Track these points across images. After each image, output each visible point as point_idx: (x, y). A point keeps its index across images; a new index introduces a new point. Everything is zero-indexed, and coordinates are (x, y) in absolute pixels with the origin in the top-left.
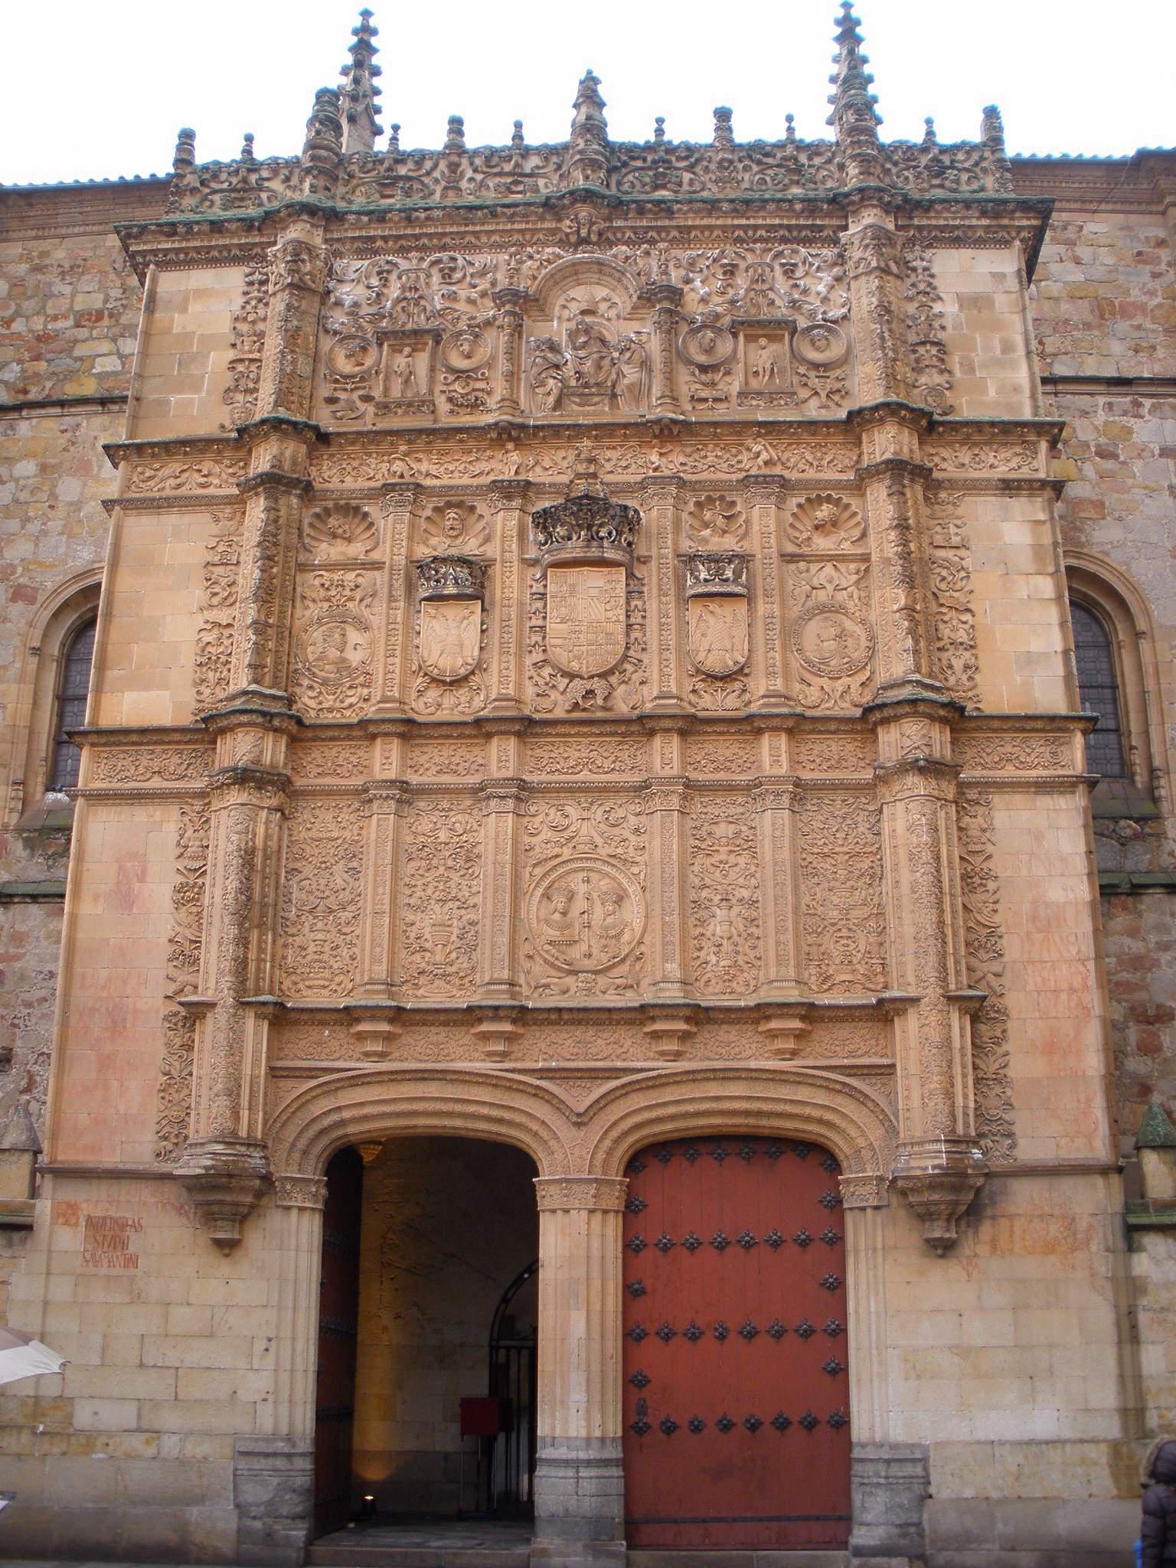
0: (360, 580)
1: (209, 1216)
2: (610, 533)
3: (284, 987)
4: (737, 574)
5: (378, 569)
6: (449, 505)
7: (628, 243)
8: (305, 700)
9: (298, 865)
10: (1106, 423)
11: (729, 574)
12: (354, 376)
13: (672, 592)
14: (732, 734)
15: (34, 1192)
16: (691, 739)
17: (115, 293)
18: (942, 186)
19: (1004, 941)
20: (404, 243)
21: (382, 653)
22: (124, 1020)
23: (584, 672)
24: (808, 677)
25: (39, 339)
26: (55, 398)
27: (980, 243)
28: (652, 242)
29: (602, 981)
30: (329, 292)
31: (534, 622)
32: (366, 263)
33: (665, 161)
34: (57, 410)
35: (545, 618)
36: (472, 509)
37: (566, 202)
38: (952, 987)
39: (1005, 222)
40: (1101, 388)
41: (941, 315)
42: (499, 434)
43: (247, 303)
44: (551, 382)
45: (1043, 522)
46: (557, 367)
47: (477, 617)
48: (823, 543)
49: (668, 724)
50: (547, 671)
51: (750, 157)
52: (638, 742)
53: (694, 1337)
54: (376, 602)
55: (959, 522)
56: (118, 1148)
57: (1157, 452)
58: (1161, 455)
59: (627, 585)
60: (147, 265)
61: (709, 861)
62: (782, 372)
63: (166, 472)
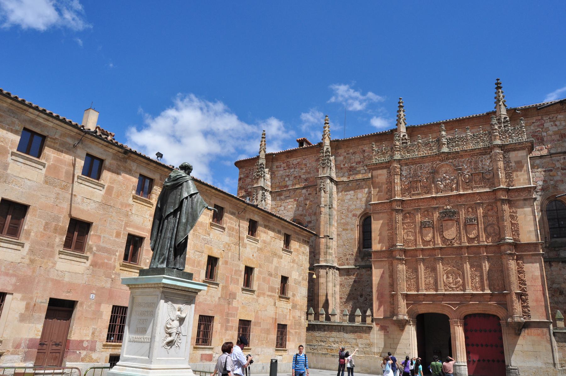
1: (399, 326)
4: (475, 221)
6: (425, 211)
7: (451, 159)
10: (563, 162)
15: (372, 321)
16: (469, 249)
17: (362, 157)
18: (511, 138)
25: (350, 167)
27: (518, 150)
28: (456, 158)
32: (407, 167)
33: (457, 141)
34: (355, 181)
39: (524, 145)
40: (562, 154)
41: (511, 166)
45: (532, 205)
47: (432, 231)
48: (490, 213)
50: (444, 239)
51: (474, 138)
53: (477, 345)
63: (379, 207)
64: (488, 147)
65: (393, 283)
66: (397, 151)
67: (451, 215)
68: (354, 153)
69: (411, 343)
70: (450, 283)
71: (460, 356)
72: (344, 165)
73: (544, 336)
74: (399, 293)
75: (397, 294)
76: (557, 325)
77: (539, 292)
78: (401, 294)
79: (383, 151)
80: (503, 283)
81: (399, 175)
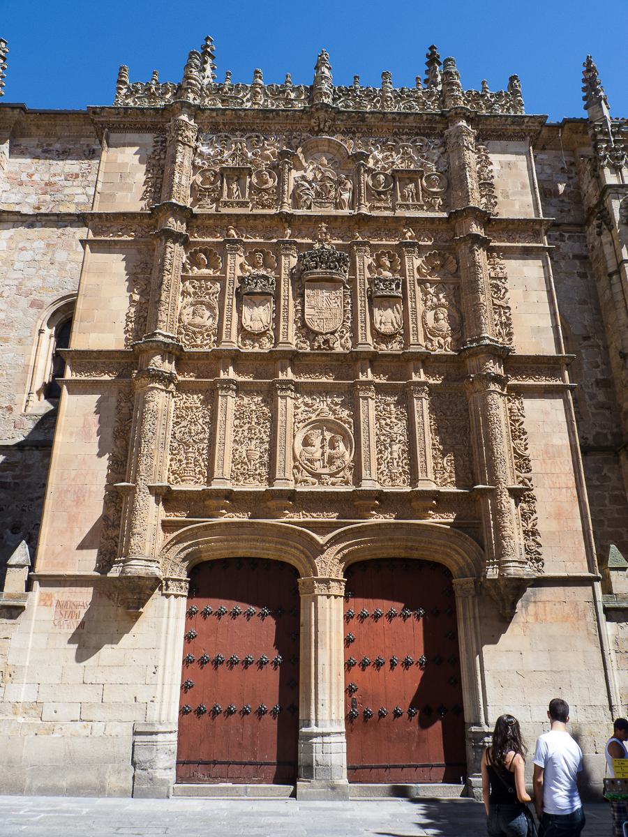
2: (336, 266)
3: (171, 480)
4: (397, 286)
6: (256, 251)
7: (343, 133)
8: (184, 340)
9: (179, 420)
11: (394, 286)
12: (210, 188)
15: (29, 587)
19: (531, 463)
22: (84, 496)
24: (431, 337)
26: (54, 212)
28: (354, 133)
29: (332, 479)
30: (196, 149)
37: (313, 109)
38: (510, 483)
39: (524, 127)
43: (155, 151)
46: (308, 189)
50: (304, 331)
55: (502, 266)
56: (77, 565)
57: (571, 257)
58: (573, 258)
60: (104, 129)
61: (383, 422)
62: (417, 194)
64: (442, 115)
65: (126, 456)
66: (193, 92)
68: (63, 153)
69: (161, 664)
70: (311, 461)
71: (327, 703)
72: (30, 176)
73: (581, 622)
74: (141, 484)
75: (134, 488)
76: (613, 585)
77: (564, 490)
78: (149, 487)
79: (150, 88)
80: (467, 463)
81: (190, 147)
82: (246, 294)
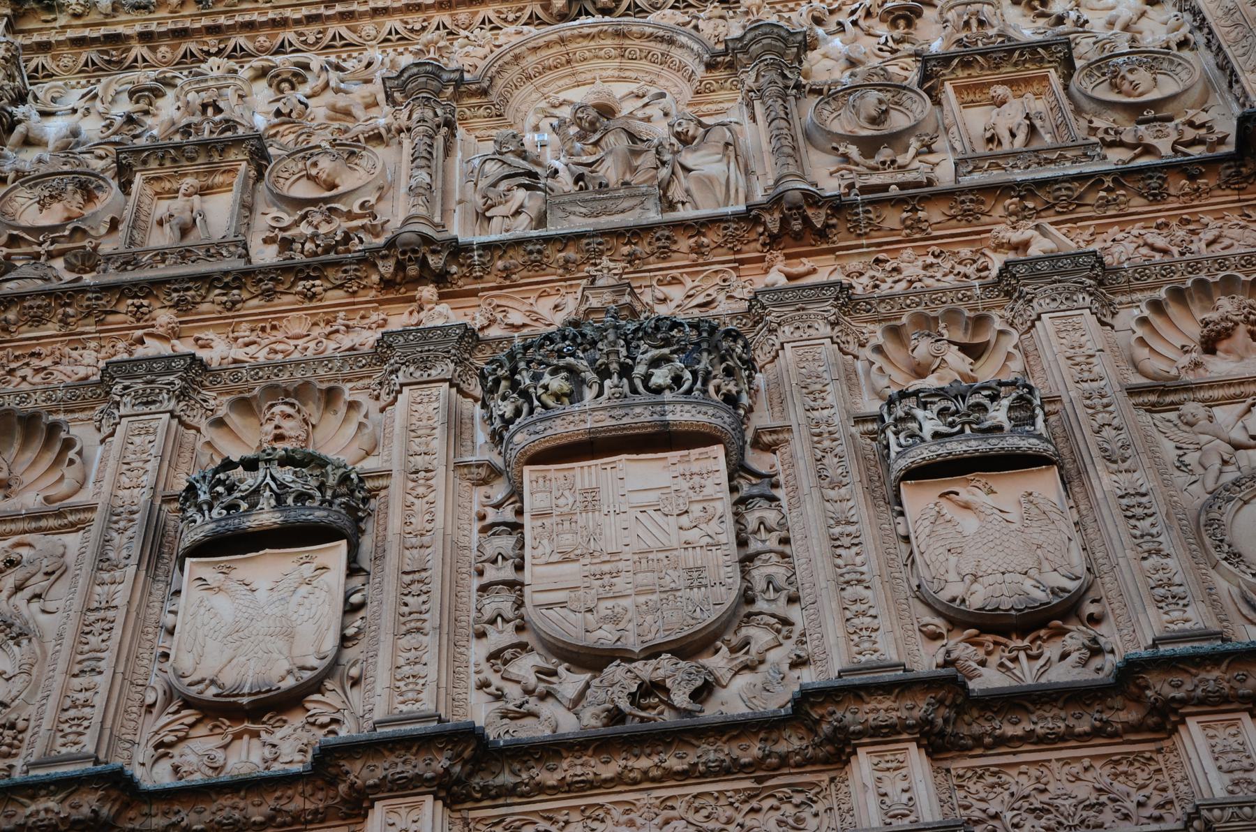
0: (25, 552)
5: (74, 527)
11: (999, 414)
13: (854, 476)
14: (1084, 738)
16: (959, 765)
20: (193, 46)
21: (62, 666)
23: (632, 642)
31: (491, 574)
35: (519, 568)
36: (330, 396)
42: (400, 266)
44: (521, 195)
46: (534, 175)
49: (881, 710)
50: (525, 667)
52: (796, 788)
54: (61, 588)
59: (733, 489)
67: (661, 376)
82: (201, 549)
